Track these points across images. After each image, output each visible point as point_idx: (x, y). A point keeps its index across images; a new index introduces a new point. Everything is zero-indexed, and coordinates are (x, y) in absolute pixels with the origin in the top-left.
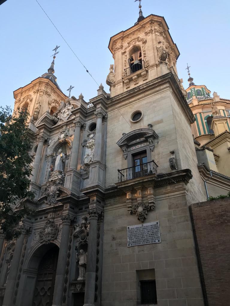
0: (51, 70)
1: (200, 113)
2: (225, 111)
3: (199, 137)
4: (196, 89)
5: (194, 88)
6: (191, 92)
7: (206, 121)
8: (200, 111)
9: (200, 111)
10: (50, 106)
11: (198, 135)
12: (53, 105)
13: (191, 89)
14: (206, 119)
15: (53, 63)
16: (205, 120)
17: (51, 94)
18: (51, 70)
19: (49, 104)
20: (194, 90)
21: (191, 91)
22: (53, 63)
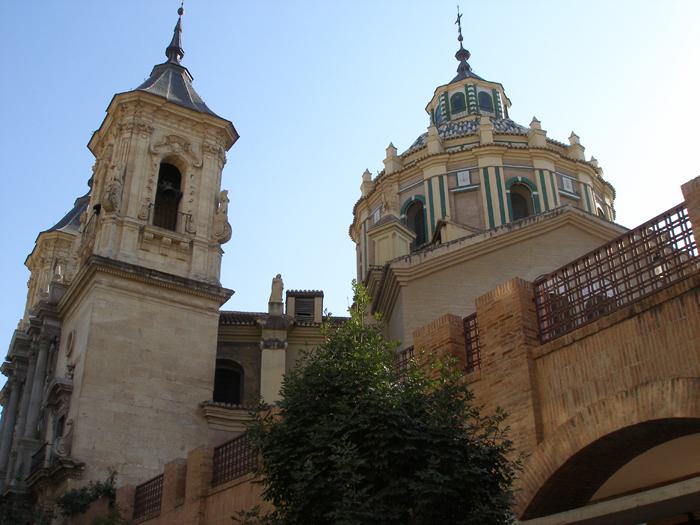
0: (174, 50)
4: (479, 90)
5: (474, 86)
6: (464, 92)
7: (508, 191)
8: (498, 162)
9: (498, 162)
10: (155, 159)
12: (165, 151)
13: (467, 87)
14: (509, 186)
15: (178, 29)
17: (153, 125)
18: (174, 50)
19: (151, 153)
20: (475, 91)
21: (467, 92)
22: (178, 29)
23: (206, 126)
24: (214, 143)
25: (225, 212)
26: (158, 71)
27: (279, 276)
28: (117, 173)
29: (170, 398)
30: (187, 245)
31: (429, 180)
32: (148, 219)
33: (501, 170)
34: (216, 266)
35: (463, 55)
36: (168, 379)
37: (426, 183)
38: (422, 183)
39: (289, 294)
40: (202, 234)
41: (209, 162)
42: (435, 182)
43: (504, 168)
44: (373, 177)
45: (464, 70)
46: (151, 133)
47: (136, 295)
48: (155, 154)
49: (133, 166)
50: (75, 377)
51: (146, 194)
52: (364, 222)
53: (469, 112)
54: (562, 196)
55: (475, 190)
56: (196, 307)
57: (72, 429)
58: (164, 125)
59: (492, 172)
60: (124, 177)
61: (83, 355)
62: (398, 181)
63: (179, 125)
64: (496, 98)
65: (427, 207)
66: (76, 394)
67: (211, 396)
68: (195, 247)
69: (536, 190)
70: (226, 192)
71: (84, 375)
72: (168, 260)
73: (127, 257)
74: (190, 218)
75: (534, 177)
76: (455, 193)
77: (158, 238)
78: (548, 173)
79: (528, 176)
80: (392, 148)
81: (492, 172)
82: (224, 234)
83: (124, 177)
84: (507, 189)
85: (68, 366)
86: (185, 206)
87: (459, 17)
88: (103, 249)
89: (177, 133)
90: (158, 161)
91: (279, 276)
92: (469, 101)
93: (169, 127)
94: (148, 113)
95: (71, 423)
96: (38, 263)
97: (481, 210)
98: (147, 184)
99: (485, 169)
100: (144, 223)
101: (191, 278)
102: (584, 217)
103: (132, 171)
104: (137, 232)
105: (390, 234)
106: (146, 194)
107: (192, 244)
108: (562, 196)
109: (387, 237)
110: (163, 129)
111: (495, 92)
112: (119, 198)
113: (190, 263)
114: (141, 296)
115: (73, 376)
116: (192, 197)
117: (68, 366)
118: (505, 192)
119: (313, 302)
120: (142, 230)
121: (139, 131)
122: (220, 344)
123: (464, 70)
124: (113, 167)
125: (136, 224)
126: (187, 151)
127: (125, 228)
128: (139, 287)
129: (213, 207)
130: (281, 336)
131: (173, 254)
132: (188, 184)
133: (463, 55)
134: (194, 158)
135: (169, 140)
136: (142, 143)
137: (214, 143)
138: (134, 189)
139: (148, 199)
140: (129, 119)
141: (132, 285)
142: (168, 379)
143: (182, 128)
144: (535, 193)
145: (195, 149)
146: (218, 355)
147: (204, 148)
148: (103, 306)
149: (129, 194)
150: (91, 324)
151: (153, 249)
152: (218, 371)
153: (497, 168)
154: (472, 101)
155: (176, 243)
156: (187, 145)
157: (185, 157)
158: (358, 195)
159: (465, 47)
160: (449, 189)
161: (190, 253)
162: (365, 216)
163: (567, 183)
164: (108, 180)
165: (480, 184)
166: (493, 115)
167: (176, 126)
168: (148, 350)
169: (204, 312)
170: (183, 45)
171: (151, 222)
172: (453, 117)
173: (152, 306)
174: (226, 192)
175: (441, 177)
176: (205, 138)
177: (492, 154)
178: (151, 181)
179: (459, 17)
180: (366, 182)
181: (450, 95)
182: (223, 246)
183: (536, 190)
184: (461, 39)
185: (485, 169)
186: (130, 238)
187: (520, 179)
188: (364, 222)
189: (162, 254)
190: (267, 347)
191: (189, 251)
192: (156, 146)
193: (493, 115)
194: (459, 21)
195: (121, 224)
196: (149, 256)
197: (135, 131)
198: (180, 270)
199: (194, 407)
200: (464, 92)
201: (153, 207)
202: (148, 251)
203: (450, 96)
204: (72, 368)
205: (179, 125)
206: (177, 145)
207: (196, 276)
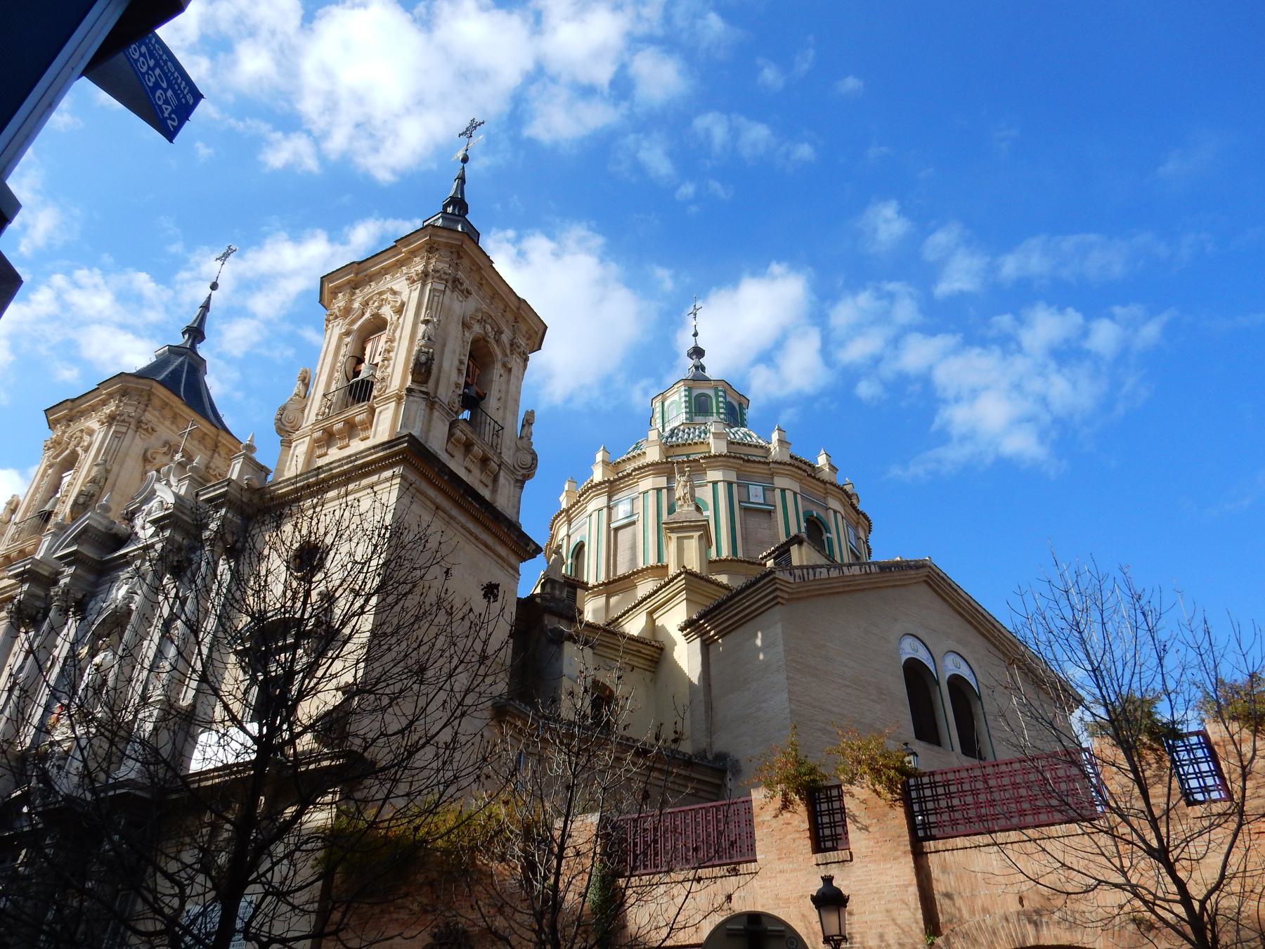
10: (467, 334)
12: (477, 328)
19: (465, 325)
40: (508, 456)
46: (467, 297)
79: (822, 514)
90: (469, 337)
104: (448, 424)
106: (454, 374)
109: (692, 537)
113: (494, 491)
114: (447, 518)
116: (499, 404)
126: (497, 341)
144: (829, 535)
145: (505, 338)
149: (440, 367)
156: (499, 332)
157: (498, 351)
177: (792, 477)
178: (461, 362)
187: (815, 515)
189: (466, 468)
198: (486, 493)
206: (488, 327)
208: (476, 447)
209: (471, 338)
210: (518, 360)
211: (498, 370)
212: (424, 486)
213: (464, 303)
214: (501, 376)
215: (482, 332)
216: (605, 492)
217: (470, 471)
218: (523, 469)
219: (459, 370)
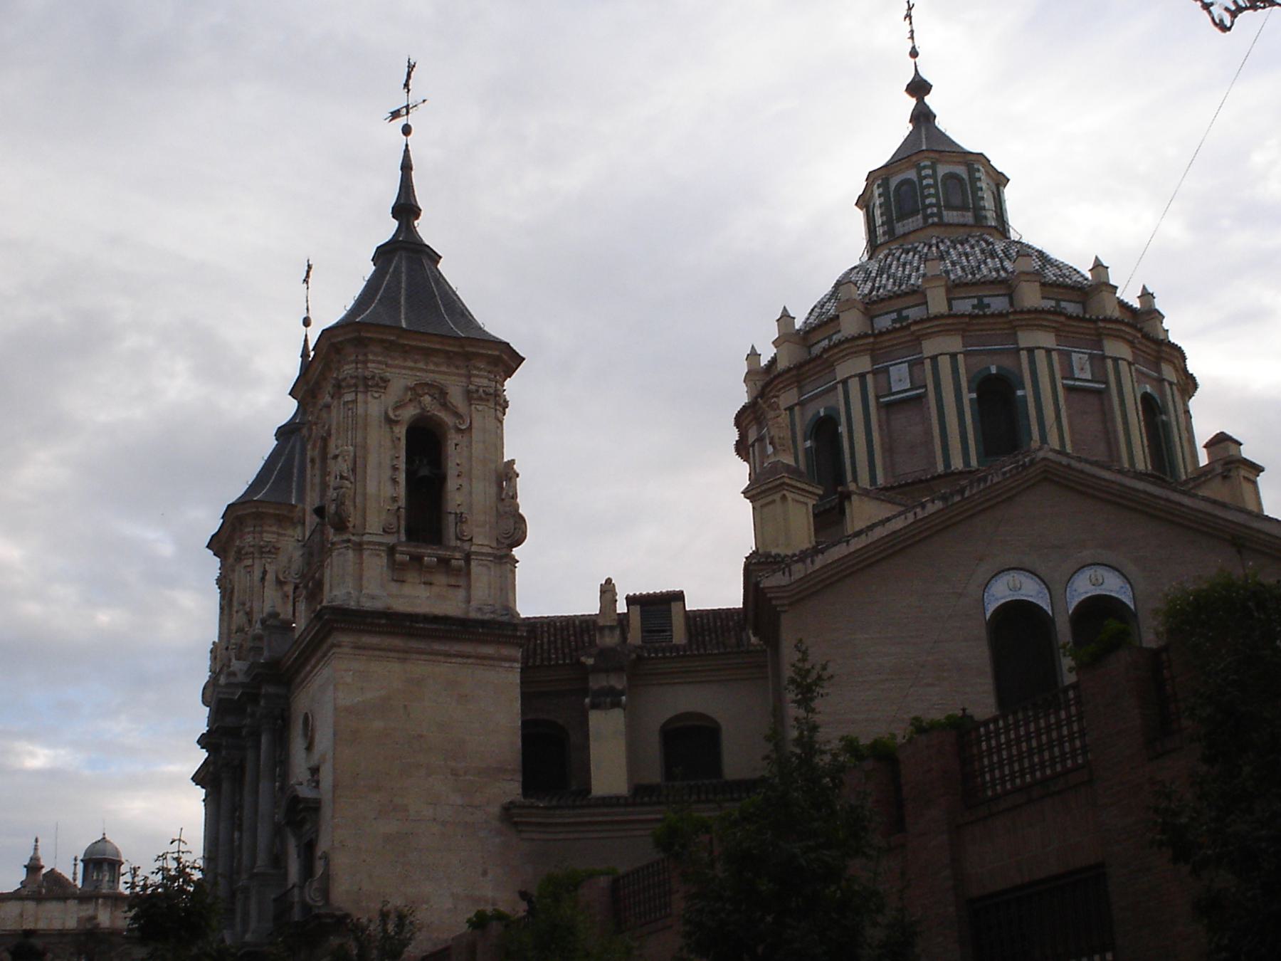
0: (406, 209)
1: (953, 356)
2: (1055, 355)
3: (940, 476)
6: (915, 179)
7: (974, 395)
8: (954, 343)
10: (397, 429)
11: (940, 468)
12: (410, 412)
15: (406, 167)
16: (970, 391)
18: (406, 209)
19: (391, 422)
20: (934, 176)
21: (921, 178)
22: (406, 167)
23: (468, 357)
24: (485, 382)
25: (514, 496)
26: (383, 255)
27: (609, 581)
28: (342, 466)
29: (459, 801)
30: (462, 562)
31: (845, 382)
32: (398, 532)
33: (960, 358)
34: (507, 586)
35: (919, 88)
36: (454, 773)
37: (840, 386)
38: (834, 388)
39: (631, 600)
40: (482, 540)
41: (480, 416)
42: (854, 385)
43: (966, 354)
44: (764, 361)
45: (922, 117)
46: (385, 388)
47: (392, 654)
48: (397, 422)
49: (365, 447)
50: (321, 785)
51: (388, 490)
52: (753, 445)
53: (926, 217)
54: (1069, 389)
55: (919, 398)
56: (484, 658)
57: (327, 865)
58: (405, 368)
59: (945, 363)
60: (354, 470)
61: (330, 754)
62: (799, 382)
63: (427, 364)
64: (974, 180)
65: (842, 429)
66: (326, 811)
67: (520, 791)
68: (473, 563)
69: (1024, 388)
70: (512, 462)
71: (335, 787)
72: (435, 589)
73: (373, 598)
74: (460, 518)
75: (1020, 364)
76: (889, 405)
77: (417, 559)
78: (1043, 352)
79: (1007, 362)
80: (785, 318)
81: (945, 363)
82: (514, 531)
83: (354, 470)
84: (970, 391)
85: (309, 769)
86: (455, 498)
87: (910, 9)
88: (339, 592)
89: (429, 378)
90: (401, 431)
91: (609, 581)
92: (924, 197)
93: (411, 369)
94: (375, 354)
95: (326, 857)
96: (232, 554)
97: (928, 432)
98: (389, 473)
99: (934, 359)
100: (390, 540)
101: (474, 615)
102: (1069, 466)
103: (365, 458)
105: (777, 497)
106: (388, 490)
107: (468, 558)
108: (1069, 389)
109: (773, 501)
110: (401, 377)
111: (971, 170)
112: (352, 509)
113: (469, 588)
114: (401, 655)
115: (318, 782)
116: (460, 482)
117: (309, 769)
118: (969, 396)
119: (670, 611)
120: (391, 550)
121: (366, 386)
122: (526, 697)
123: (922, 117)
124: (336, 457)
125: (380, 544)
127: (366, 553)
128: (398, 642)
129: (493, 490)
130: (618, 682)
131: (441, 579)
132: (455, 456)
133: (919, 88)
134: (457, 415)
135: (415, 391)
136: (373, 406)
137: (485, 382)
138: (372, 488)
139: (394, 499)
140: (348, 369)
141: (388, 641)
142: (454, 773)
143: (432, 367)
144: (1020, 393)
145: (456, 396)
146: (523, 712)
147: (469, 396)
148: (349, 680)
149: (365, 495)
150: (336, 709)
151: (411, 576)
152: (526, 738)
153: (953, 356)
154: (930, 195)
155: (444, 563)
156: (441, 394)
158: (740, 397)
159: (925, 74)
160: (877, 397)
161: (468, 574)
162: (752, 436)
163: (1080, 360)
164: (332, 481)
165: (925, 386)
166: (969, 217)
167: (421, 365)
168: (421, 736)
169: (496, 663)
170: (421, 199)
171: (403, 538)
172: (900, 228)
173: (419, 668)
174: (512, 462)
175: (862, 376)
176: (469, 376)
178: (395, 469)
179: (910, 9)
180: (752, 376)
181: (894, 182)
182: (516, 552)
183: (1024, 388)
184: (914, 53)
185: (934, 359)
186: (376, 566)
188: (753, 445)
189: (425, 583)
190: (595, 706)
191: (465, 572)
192: (396, 408)
193: (969, 217)
194: (909, 16)
195: (359, 547)
196: (407, 589)
197: (361, 388)
199: (495, 810)
200: (915, 179)
201: (403, 511)
202: (403, 581)
203: (892, 188)
204: (315, 771)
205: (427, 364)
206: (427, 399)
207: (480, 609)
208: (426, 558)
209: (404, 431)
210: (480, 408)
211: (453, 438)
212: (367, 640)
213: (383, 397)
214: (456, 445)
215: (418, 411)
216: (751, 421)
217: (431, 584)
218: (508, 538)
219: (394, 481)
